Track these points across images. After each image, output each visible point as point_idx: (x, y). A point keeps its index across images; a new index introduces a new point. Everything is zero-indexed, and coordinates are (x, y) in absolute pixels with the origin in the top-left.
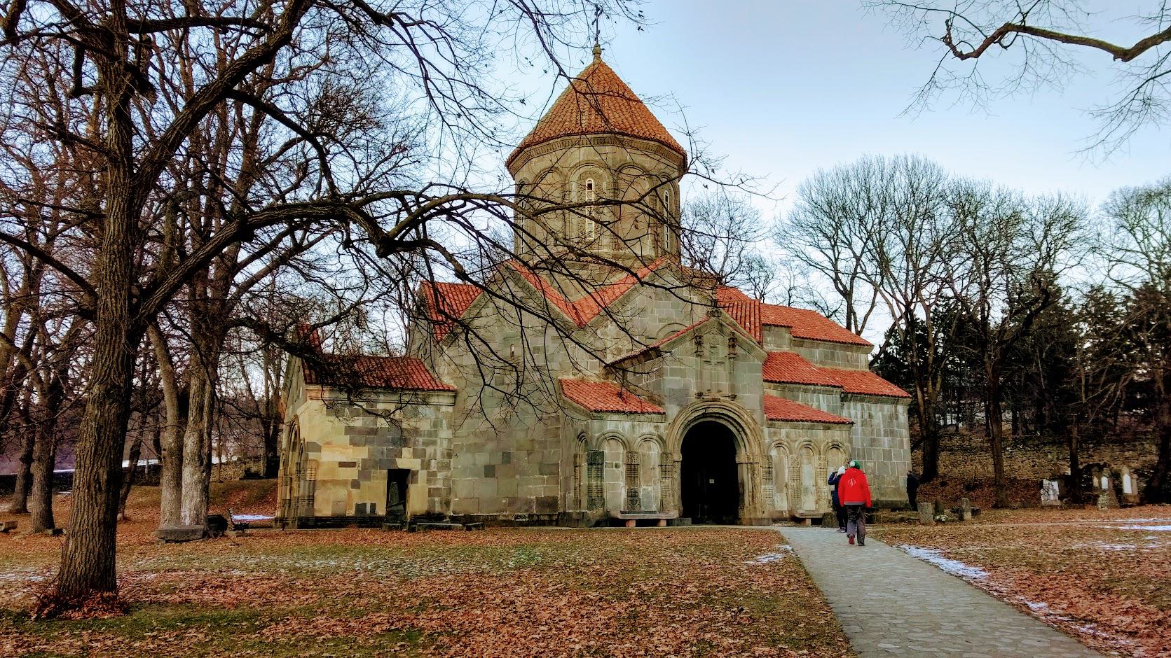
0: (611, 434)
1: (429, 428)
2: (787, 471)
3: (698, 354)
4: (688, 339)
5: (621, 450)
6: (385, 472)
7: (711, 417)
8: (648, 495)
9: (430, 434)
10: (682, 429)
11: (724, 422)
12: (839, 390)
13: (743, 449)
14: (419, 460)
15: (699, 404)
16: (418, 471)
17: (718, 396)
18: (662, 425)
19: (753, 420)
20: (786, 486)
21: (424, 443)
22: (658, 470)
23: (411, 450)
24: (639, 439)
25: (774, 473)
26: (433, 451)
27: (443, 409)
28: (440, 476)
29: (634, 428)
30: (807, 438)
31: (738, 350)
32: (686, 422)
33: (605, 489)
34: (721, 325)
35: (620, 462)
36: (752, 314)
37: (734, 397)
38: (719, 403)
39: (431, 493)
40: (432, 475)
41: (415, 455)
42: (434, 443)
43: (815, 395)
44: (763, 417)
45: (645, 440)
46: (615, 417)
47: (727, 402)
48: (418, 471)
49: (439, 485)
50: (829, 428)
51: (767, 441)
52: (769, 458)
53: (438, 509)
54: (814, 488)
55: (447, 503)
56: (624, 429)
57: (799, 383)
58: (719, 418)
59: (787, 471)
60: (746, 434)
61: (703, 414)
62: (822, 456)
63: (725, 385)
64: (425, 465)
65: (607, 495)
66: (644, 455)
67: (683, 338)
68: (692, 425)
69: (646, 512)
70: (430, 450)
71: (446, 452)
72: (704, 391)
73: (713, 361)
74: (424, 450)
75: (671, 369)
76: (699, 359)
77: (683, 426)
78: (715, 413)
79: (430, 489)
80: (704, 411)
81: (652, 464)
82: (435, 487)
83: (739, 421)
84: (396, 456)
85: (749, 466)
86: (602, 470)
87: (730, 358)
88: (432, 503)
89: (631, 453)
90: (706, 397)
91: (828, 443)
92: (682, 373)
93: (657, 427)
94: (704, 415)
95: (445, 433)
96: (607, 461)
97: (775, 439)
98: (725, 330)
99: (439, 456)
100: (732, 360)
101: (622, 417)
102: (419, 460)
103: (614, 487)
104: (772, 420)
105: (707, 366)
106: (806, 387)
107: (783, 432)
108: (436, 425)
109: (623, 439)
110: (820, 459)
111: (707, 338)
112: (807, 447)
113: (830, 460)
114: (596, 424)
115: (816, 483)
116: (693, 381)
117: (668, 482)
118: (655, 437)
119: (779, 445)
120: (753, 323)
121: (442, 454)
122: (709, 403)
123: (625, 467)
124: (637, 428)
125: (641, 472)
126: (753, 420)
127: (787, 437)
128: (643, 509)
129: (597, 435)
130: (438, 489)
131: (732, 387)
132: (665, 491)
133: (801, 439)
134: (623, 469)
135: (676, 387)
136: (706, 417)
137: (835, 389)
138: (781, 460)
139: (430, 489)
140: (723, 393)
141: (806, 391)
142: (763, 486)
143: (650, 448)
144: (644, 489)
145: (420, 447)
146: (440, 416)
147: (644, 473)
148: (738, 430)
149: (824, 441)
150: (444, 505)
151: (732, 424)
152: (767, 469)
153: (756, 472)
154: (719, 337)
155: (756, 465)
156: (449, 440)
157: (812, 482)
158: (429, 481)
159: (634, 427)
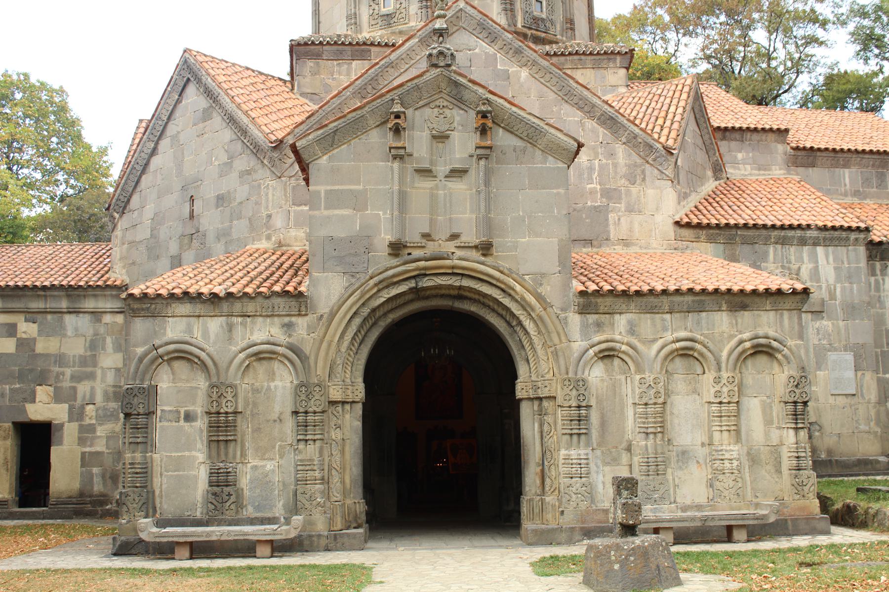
0: (172, 347)
1: (81, 351)
2: (630, 412)
3: (399, 155)
4: (372, 122)
5: (202, 383)
6: (8, 425)
7: (442, 296)
8: (263, 482)
9: (84, 361)
10: (354, 328)
11: (473, 308)
12: (862, 236)
13: (522, 370)
14: (66, 406)
15: (396, 267)
16: (62, 426)
17: (450, 247)
18: (302, 323)
20: (629, 449)
21: (73, 378)
22: (289, 424)
23: (51, 389)
24: (242, 356)
26: (88, 389)
27: (107, 319)
28: (101, 431)
29: (230, 331)
30: (683, 334)
31: (501, 138)
32: (366, 311)
33: (157, 469)
34: (456, 84)
35: (198, 409)
36: (675, 101)
37: (486, 248)
38: (447, 262)
39: (87, 460)
40: (86, 433)
41: (58, 398)
42: (91, 376)
43: (806, 248)
44: (567, 286)
45: (259, 356)
47: (473, 262)
48: (62, 426)
49: (100, 446)
50: (744, 307)
51: (578, 345)
52: (579, 384)
53: (98, 487)
54: (706, 450)
55: (114, 478)
56: (206, 334)
57: (765, 226)
58: (460, 297)
59: (630, 412)
60: (527, 333)
61: (411, 289)
62: (725, 375)
64: (76, 414)
65: (161, 483)
66: (256, 391)
67: (356, 121)
68: (392, 317)
69: (252, 521)
70: (83, 388)
71: (111, 389)
72: (413, 236)
73: (442, 169)
74: (74, 389)
75: (326, 192)
76: (396, 165)
77: (357, 321)
78: (440, 287)
79: (83, 454)
80: (412, 284)
81: (277, 409)
82: (93, 449)
83: (506, 301)
84: (25, 400)
85: (536, 403)
86: (146, 429)
87: (480, 158)
88: (88, 479)
89: (218, 389)
90: (417, 253)
91: (741, 342)
92: (358, 201)
93: (289, 326)
94: (417, 293)
95: (110, 360)
96: (164, 406)
97: (596, 339)
98: (467, 96)
99: (99, 398)
100: (482, 162)
101: (199, 308)
102: (66, 406)
103: (179, 464)
104: (583, 294)
105: (426, 184)
106: (783, 233)
107: (621, 321)
108: (95, 345)
109: (203, 355)
110: (717, 380)
112: (685, 354)
113: (749, 380)
114: (140, 326)
115: (711, 437)
116: (384, 215)
117: (311, 450)
118: (279, 349)
119: (607, 355)
120: (670, 116)
121: (106, 393)
122: (422, 264)
123: (206, 419)
124: (238, 331)
125: (245, 427)
126: (539, 298)
127: (632, 331)
128: (250, 511)
129: (140, 350)
130: (98, 453)
132: (304, 465)
133: (669, 337)
134: (201, 423)
135: (340, 233)
136: (427, 298)
137: (853, 236)
138: (614, 388)
139: (83, 454)
140: (463, 238)
141: (784, 241)
142: (563, 452)
143: (272, 376)
144: (255, 468)
145: (66, 384)
146: (102, 330)
147: (257, 430)
148: (509, 324)
149: (732, 337)
150: (109, 482)
151: (493, 310)
152: (575, 412)
153: (549, 419)
154: (457, 115)
155: (545, 403)
156: (118, 370)
157: (700, 437)
158: (82, 441)
159: (230, 328)
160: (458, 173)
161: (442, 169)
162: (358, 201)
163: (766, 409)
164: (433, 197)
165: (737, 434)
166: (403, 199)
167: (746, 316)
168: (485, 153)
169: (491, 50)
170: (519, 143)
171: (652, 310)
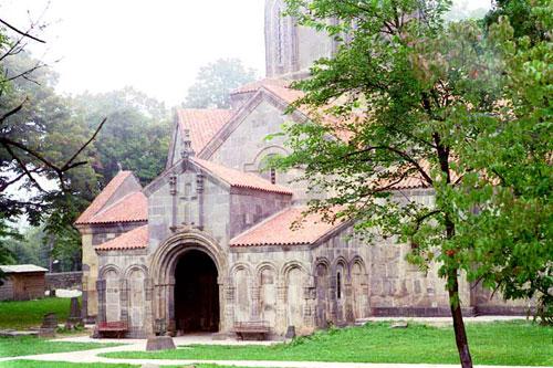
2: (249, 290)
3: (174, 193)
18: (146, 257)
19: (218, 247)
22: (143, 294)
25: (237, 292)
35: (118, 288)
37: (201, 228)
46: (112, 252)
63: (196, 215)
72: (179, 224)
92: (162, 211)
93: (142, 259)
105: (184, 203)
107: (246, 255)
111: (182, 178)
116: (169, 216)
119: (241, 268)
126: (218, 247)
131: (202, 219)
160: (194, 198)
161: (190, 197)
162: (162, 211)
163: (298, 290)
164: (186, 207)
165: (286, 300)
166: (175, 211)
167: (289, 253)
168: (201, 191)
169: (276, 109)
170: (213, 185)
171: (255, 251)
